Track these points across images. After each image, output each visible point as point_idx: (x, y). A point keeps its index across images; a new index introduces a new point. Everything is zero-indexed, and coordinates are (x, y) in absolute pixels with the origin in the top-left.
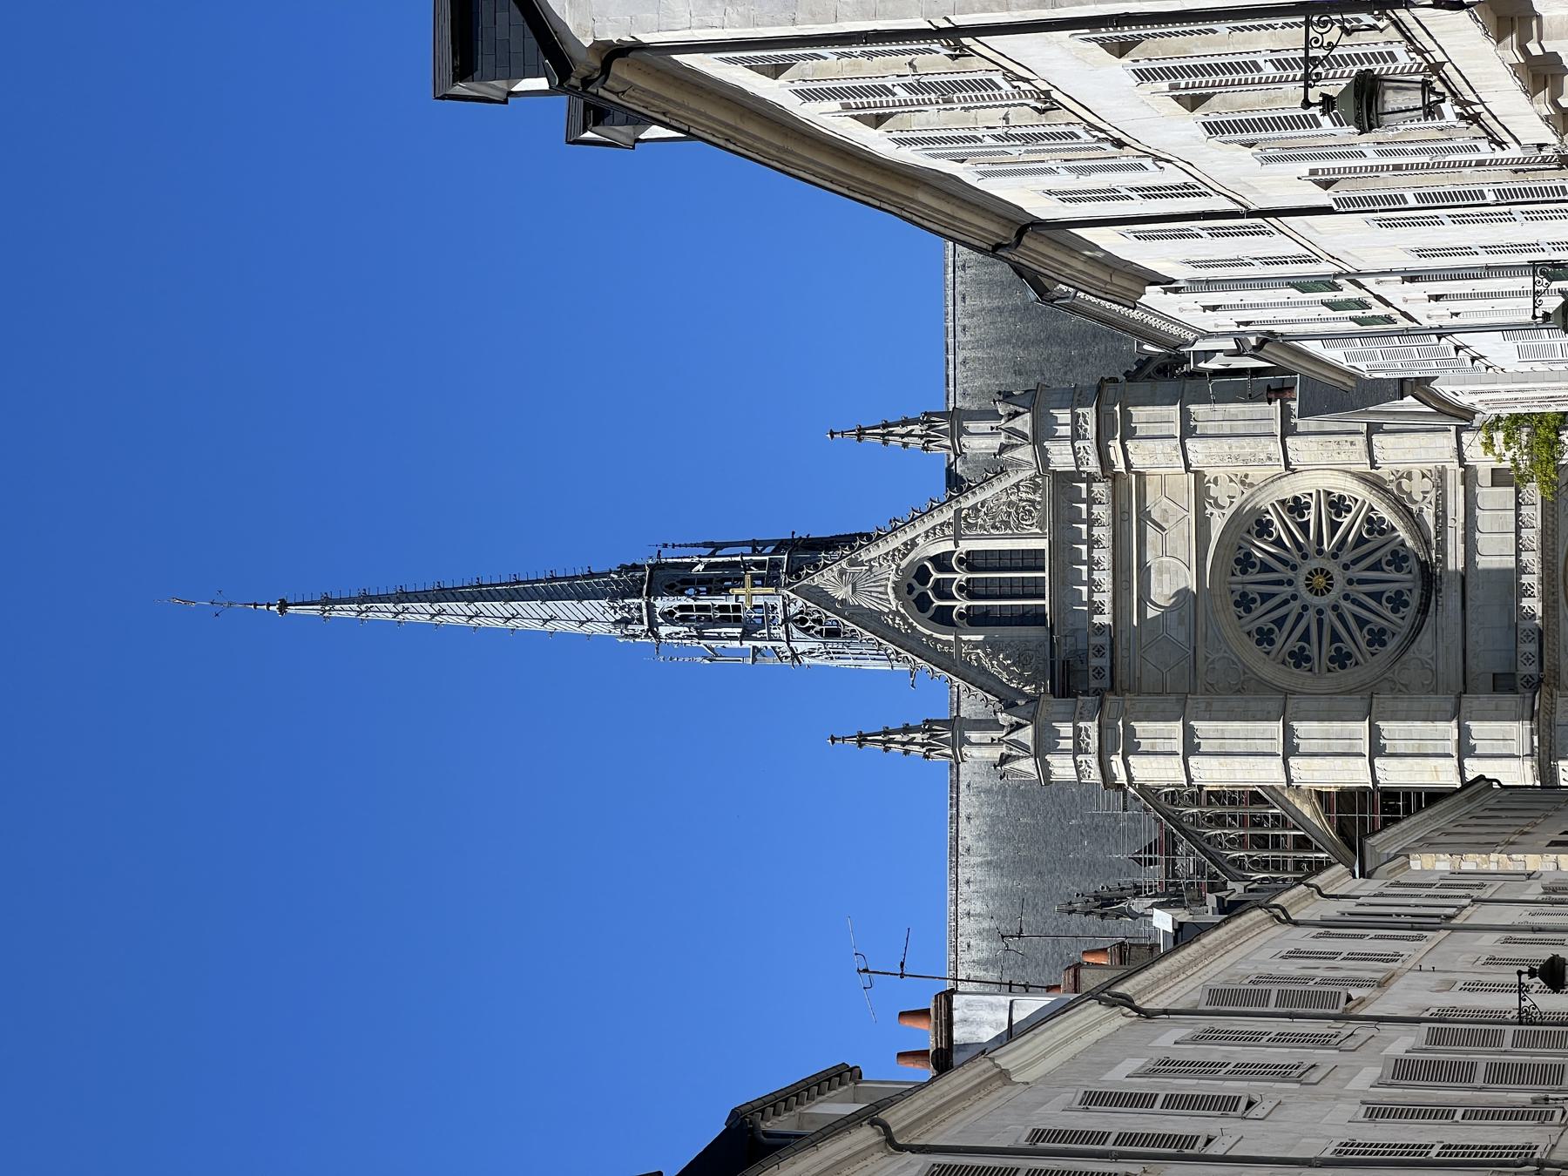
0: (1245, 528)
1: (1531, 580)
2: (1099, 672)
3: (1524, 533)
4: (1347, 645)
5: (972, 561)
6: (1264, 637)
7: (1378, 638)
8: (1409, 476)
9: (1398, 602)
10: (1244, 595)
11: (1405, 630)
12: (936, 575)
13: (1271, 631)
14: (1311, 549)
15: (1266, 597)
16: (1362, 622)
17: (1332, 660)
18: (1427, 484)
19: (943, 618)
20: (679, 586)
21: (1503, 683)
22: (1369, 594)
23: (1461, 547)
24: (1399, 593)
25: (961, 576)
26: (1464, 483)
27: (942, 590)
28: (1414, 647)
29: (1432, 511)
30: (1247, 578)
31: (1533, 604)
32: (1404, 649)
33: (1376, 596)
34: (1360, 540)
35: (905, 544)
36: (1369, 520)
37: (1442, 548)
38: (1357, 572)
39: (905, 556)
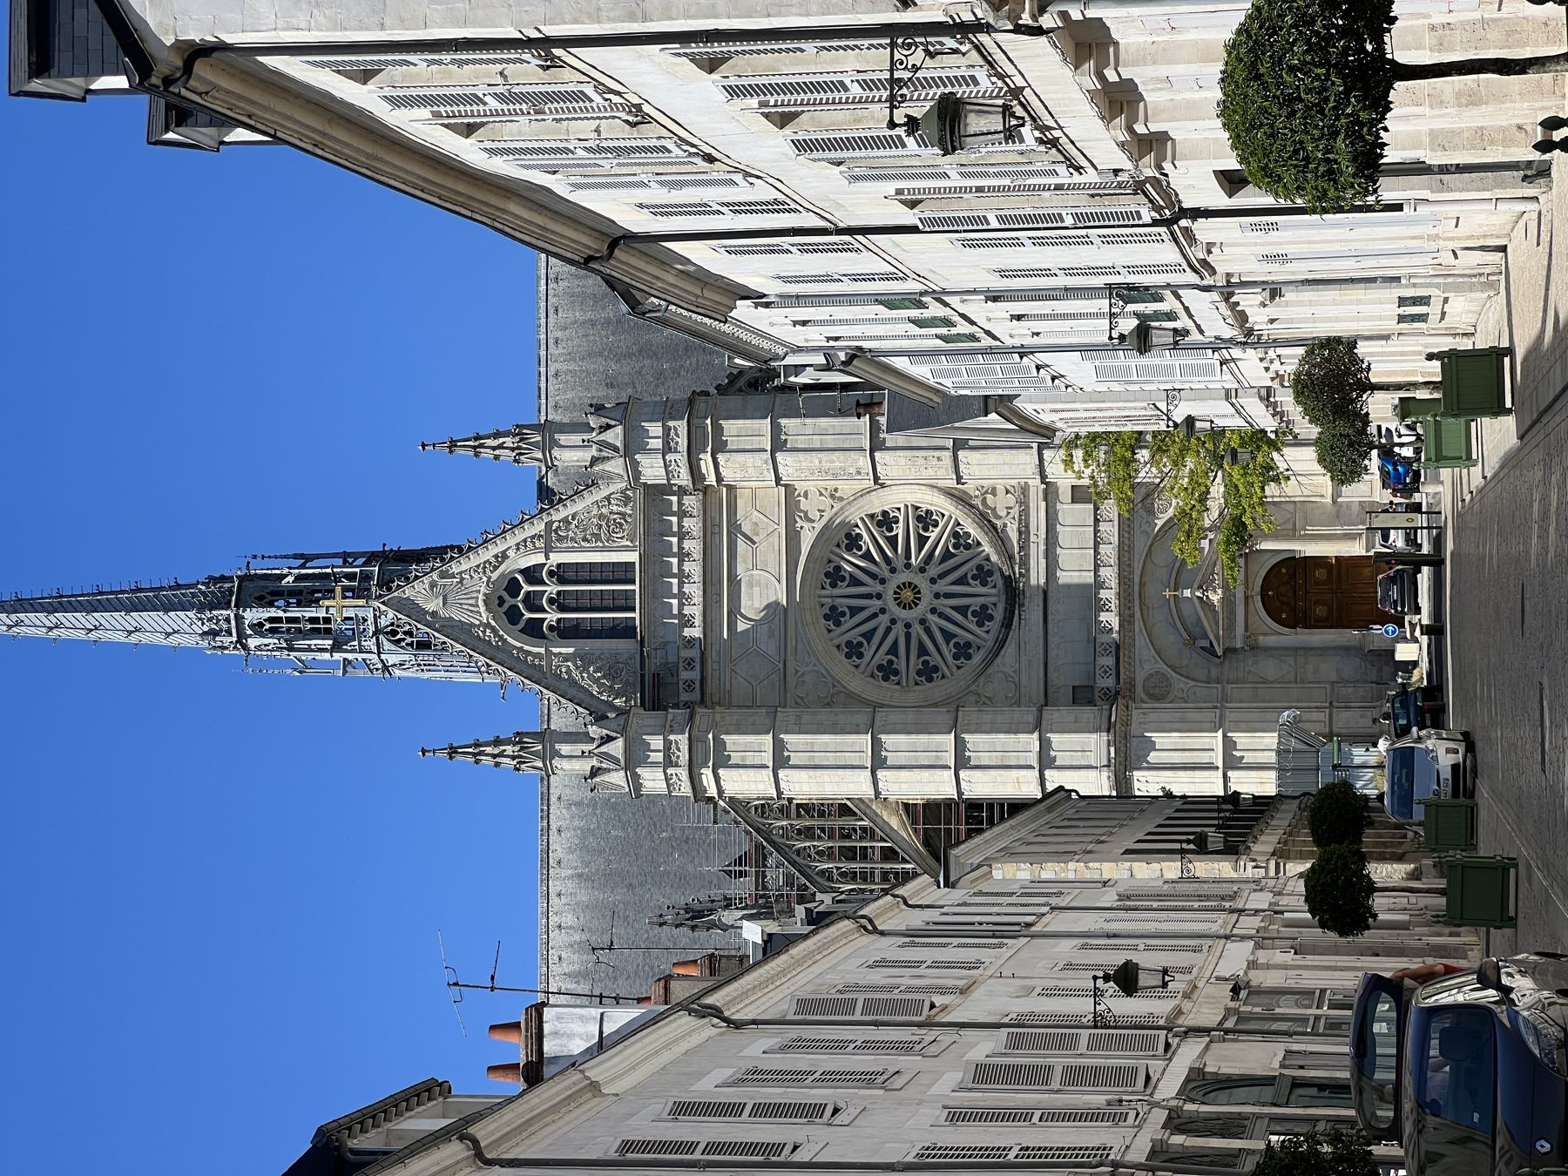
1: (1109, 595)
2: (689, 685)
3: (1103, 549)
4: (935, 659)
5: (562, 574)
6: (853, 650)
7: (963, 651)
8: (994, 492)
9: (983, 615)
10: (833, 608)
11: (990, 643)
12: (526, 588)
13: (860, 644)
14: (899, 563)
15: (855, 611)
16: (948, 636)
17: (919, 673)
19: (534, 630)
20: (269, 598)
21: (1082, 696)
23: (1043, 562)
24: (984, 607)
25: (552, 589)
26: (1046, 499)
27: (532, 602)
29: (1015, 527)
30: (836, 591)
31: (1110, 619)
32: (989, 662)
33: (962, 610)
34: (947, 555)
35: (496, 556)
36: (956, 535)
37: (1025, 562)
38: (943, 586)
39: (496, 568)
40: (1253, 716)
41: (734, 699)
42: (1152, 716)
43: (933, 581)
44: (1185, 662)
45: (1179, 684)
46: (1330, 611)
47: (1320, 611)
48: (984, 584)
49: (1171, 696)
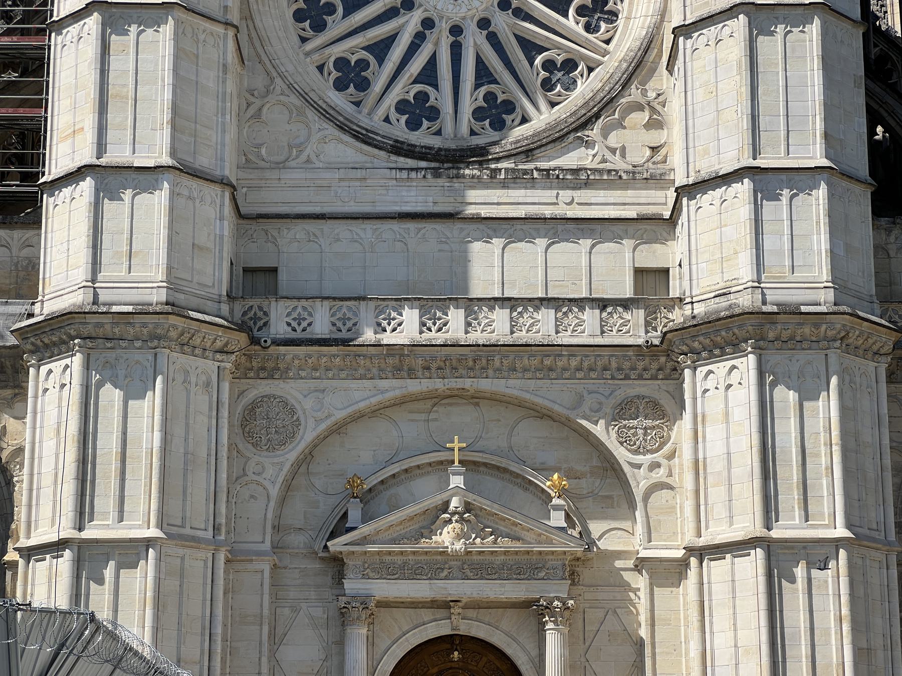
1: (455, 325)
3: (547, 316)
7: (351, 76)
8: (655, 124)
9: (418, 111)
11: (365, 122)
16: (381, 49)
18: (639, 155)
21: (256, 280)
22: (432, 61)
23: (520, 212)
24: (434, 114)
26: (641, 219)
28: (331, 130)
29: (588, 163)
31: (407, 327)
32: (327, 114)
33: (429, 74)
34: (531, 48)
36: (570, 65)
37: (517, 179)
38: (474, 41)
40: (196, 607)
42: (202, 401)
44: (318, 483)
45: (273, 468)
48: (478, 114)
49: (247, 448)
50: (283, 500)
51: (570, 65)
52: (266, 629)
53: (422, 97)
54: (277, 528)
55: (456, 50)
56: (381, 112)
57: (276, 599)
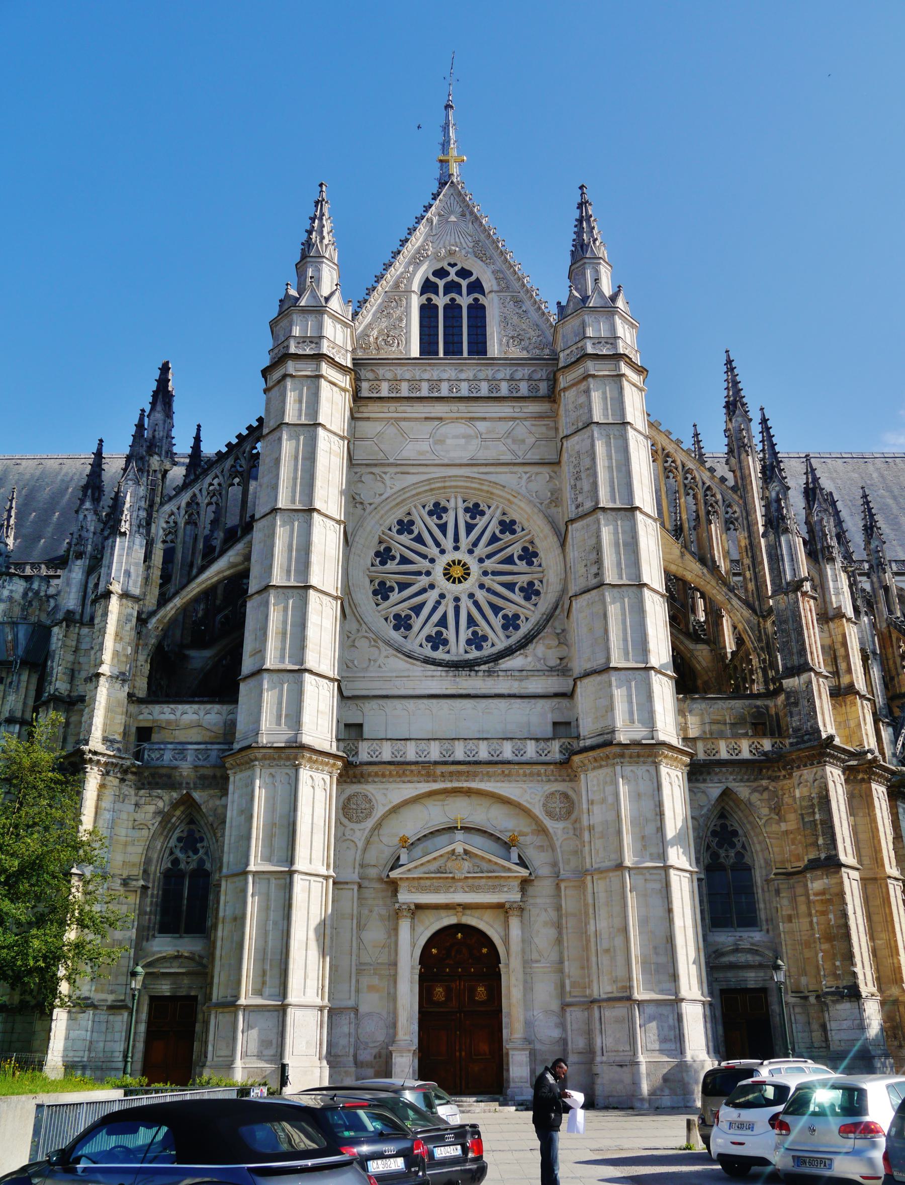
0: (507, 509)
4: (395, 596)
7: (402, 623)
10: (445, 510)
12: (464, 283)
15: (443, 528)
16: (417, 609)
19: (428, 287)
24: (445, 642)
25: (465, 301)
30: (461, 512)
33: (443, 622)
38: (466, 604)
41: (360, 424)
43: (471, 596)
46: (438, 1004)
47: (439, 992)
48: (469, 642)
49: (345, 821)
50: (365, 850)
51: (516, 616)
52: (355, 921)
53: (439, 634)
54: (362, 866)
55: (457, 610)
56: (418, 641)
57: (361, 905)
